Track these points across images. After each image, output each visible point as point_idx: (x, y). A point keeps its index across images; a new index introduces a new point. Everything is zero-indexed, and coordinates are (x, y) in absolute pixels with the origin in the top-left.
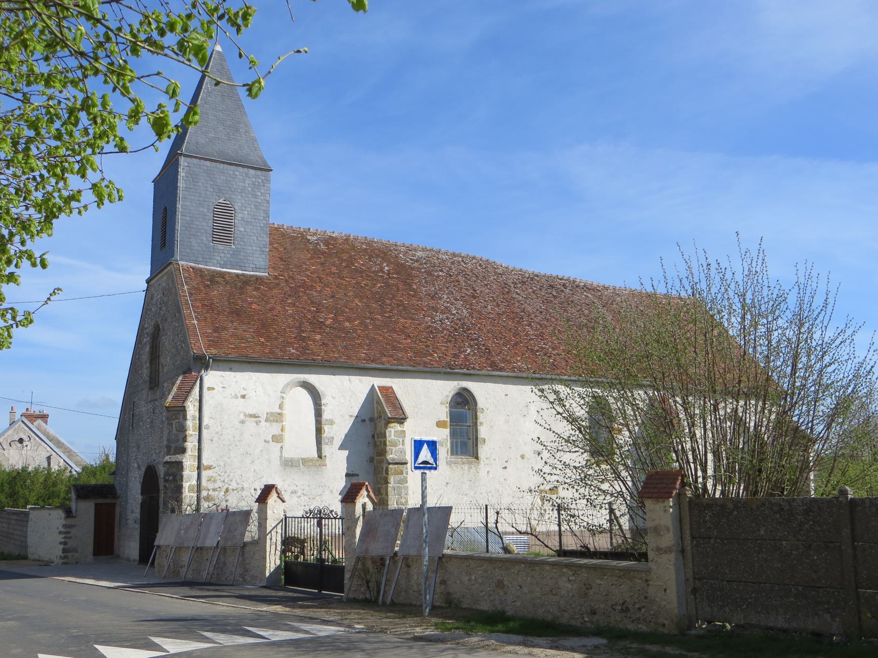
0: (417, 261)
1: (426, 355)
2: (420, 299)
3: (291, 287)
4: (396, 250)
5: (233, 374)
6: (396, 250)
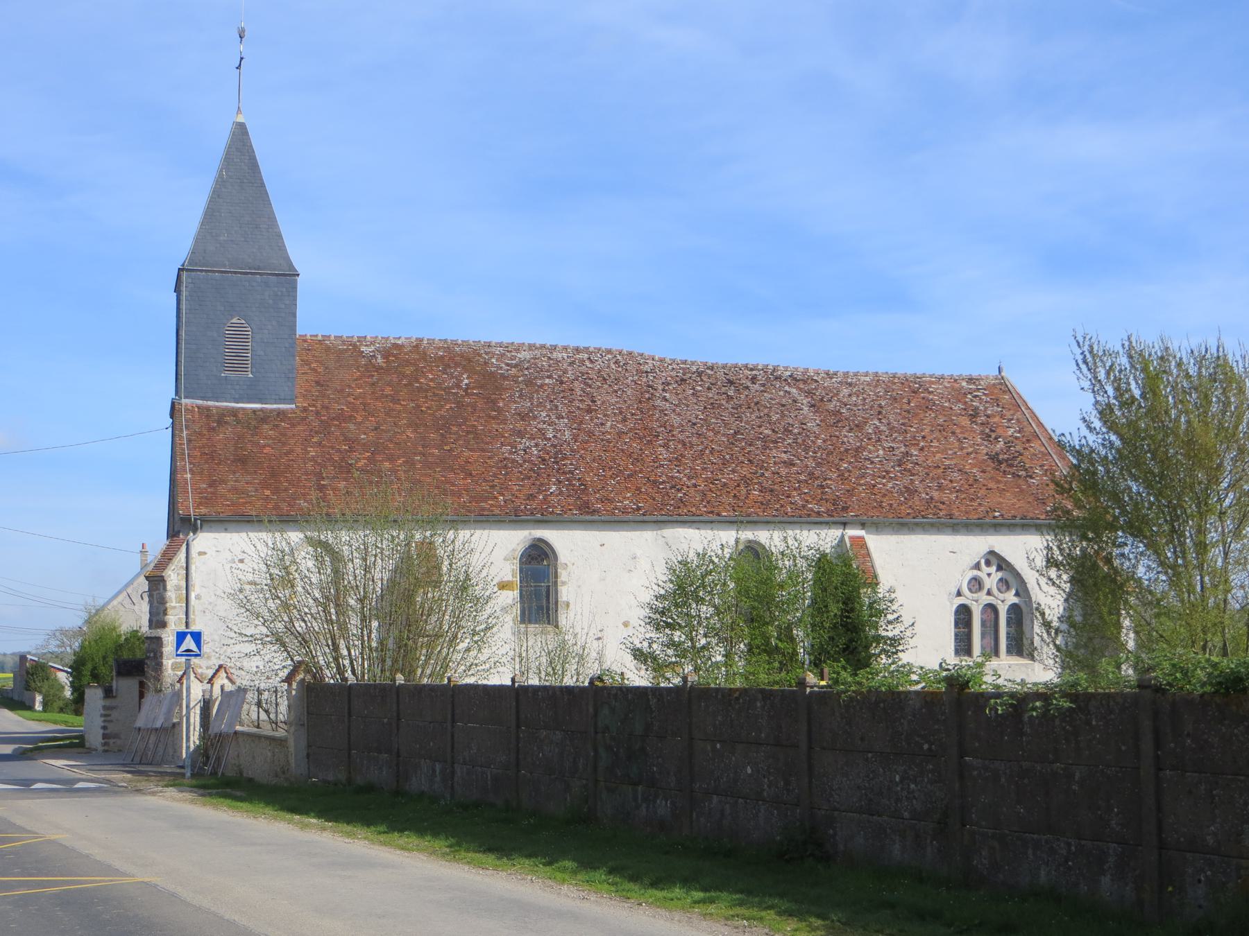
0: (516, 366)
1: (485, 499)
2: (504, 422)
3: (322, 421)
4: (487, 353)
5: (228, 535)
6: (487, 353)
